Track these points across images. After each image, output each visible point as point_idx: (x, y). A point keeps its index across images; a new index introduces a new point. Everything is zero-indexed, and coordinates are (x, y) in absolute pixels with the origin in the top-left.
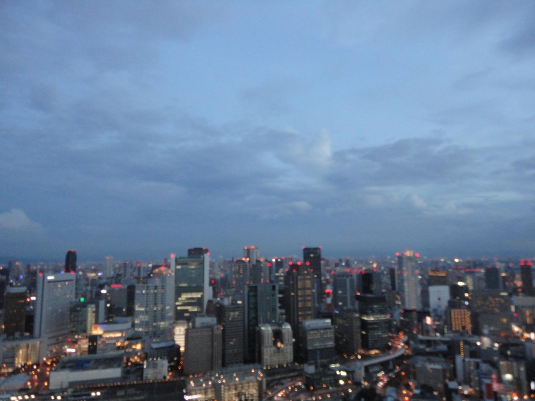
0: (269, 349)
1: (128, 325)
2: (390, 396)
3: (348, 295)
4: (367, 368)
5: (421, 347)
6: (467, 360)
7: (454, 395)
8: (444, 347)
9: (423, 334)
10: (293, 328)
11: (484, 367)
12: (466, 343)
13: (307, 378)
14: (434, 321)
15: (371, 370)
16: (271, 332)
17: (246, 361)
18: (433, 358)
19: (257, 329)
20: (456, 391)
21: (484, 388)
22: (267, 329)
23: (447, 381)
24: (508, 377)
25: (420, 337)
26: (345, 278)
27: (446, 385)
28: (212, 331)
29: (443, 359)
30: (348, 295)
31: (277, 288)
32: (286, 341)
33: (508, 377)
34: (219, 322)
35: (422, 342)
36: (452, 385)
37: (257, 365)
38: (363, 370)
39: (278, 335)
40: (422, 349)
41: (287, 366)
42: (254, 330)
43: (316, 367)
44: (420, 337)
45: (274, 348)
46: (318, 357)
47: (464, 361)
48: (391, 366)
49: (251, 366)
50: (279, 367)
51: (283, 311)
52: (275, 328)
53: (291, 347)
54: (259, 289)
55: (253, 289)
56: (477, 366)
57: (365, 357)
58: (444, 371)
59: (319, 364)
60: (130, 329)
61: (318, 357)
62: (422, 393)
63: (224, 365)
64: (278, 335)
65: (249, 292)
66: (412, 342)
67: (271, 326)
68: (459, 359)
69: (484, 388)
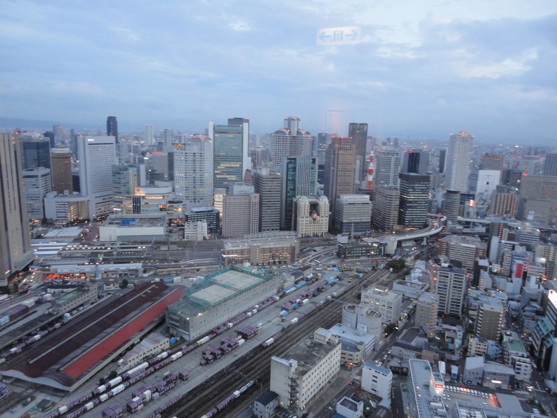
0: (305, 219)
1: (170, 189)
2: (418, 268)
3: (392, 174)
4: (400, 243)
5: (459, 227)
6: (503, 241)
7: (482, 271)
8: (483, 230)
9: (463, 216)
10: (331, 202)
11: (520, 250)
12: (506, 226)
13: (339, 246)
14: (476, 204)
15: (403, 245)
16: (307, 203)
17: (281, 229)
18: (468, 238)
19: (295, 200)
20: (485, 268)
21: (515, 268)
22: (304, 202)
23: (478, 259)
24: (543, 260)
25: (460, 218)
26: (390, 156)
27: (476, 263)
28: (250, 199)
29: (479, 240)
30: (392, 174)
31: (317, 163)
32: (322, 213)
33: (543, 260)
34: (257, 191)
35: (460, 222)
36: (483, 263)
37: (292, 233)
38: (396, 244)
39: (314, 207)
40: (459, 229)
41: (322, 236)
42: (292, 201)
43: (349, 238)
44: (460, 218)
45: (310, 219)
46: (353, 229)
47: (500, 242)
48: (424, 243)
49: (286, 233)
50: (314, 235)
51: (322, 186)
52: (313, 200)
53: (328, 218)
54: (298, 161)
55: (292, 161)
56: (513, 248)
57: (398, 233)
58: (477, 249)
59: (352, 235)
60: (171, 193)
61: (353, 229)
62: (449, 267)
63: (260, 230)
64: (314, 207)
65: (288, 163)
66: (450, 223)
67: (308, 198)
68: (495, 241)
69: (515, 268)
